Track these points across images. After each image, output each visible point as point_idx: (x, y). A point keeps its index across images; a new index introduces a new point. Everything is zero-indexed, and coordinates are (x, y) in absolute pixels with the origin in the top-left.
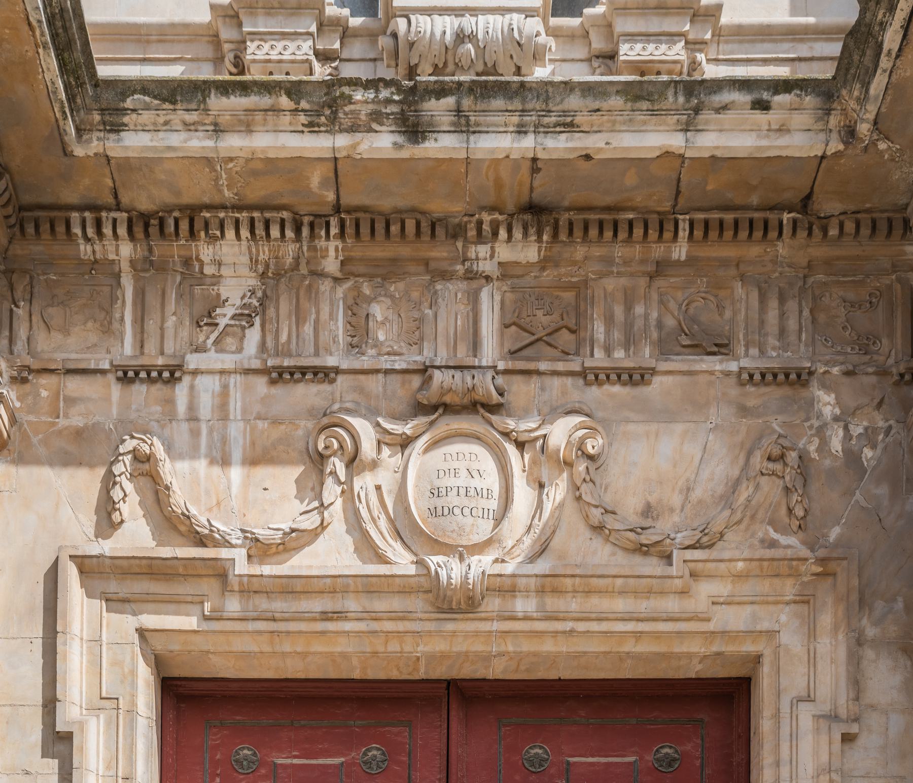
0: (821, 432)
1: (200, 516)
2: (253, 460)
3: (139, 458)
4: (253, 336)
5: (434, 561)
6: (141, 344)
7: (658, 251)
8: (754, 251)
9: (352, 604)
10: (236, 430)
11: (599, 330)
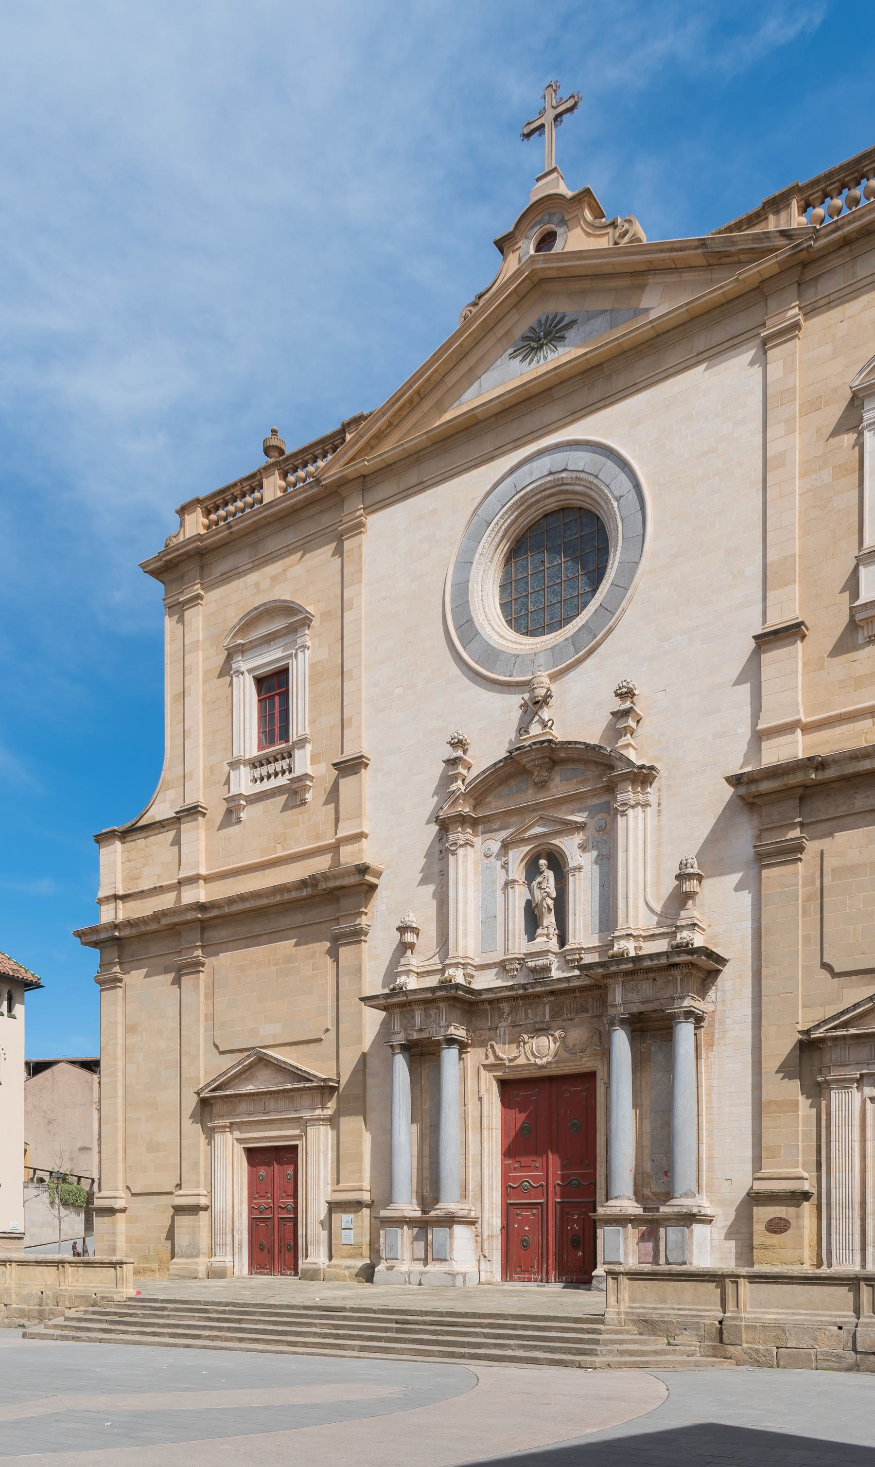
0: (604, 1026)
1: (500, 1054)
2: (509, 1043)
3: (491, 1045)
4: (510, 1018)
5: (537, 1060)
6: (491, 1023)
7: (574, 995)
8: (591, 993)
9: (526, 1068)
10: (507, 1037)
11: (565, 1011)
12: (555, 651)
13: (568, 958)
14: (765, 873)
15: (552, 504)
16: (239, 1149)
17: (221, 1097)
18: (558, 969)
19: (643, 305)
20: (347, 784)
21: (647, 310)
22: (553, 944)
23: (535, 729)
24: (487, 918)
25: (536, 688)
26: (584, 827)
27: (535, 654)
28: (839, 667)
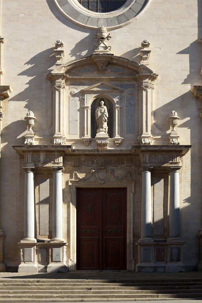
12: (108, 21)
13: (116, 142)
18: (110, 147)
22: (107, 136)
23: (101, 49)
24: (72, 120)
25: (103, 32)
26: (123, 92)
27: (98, 19)
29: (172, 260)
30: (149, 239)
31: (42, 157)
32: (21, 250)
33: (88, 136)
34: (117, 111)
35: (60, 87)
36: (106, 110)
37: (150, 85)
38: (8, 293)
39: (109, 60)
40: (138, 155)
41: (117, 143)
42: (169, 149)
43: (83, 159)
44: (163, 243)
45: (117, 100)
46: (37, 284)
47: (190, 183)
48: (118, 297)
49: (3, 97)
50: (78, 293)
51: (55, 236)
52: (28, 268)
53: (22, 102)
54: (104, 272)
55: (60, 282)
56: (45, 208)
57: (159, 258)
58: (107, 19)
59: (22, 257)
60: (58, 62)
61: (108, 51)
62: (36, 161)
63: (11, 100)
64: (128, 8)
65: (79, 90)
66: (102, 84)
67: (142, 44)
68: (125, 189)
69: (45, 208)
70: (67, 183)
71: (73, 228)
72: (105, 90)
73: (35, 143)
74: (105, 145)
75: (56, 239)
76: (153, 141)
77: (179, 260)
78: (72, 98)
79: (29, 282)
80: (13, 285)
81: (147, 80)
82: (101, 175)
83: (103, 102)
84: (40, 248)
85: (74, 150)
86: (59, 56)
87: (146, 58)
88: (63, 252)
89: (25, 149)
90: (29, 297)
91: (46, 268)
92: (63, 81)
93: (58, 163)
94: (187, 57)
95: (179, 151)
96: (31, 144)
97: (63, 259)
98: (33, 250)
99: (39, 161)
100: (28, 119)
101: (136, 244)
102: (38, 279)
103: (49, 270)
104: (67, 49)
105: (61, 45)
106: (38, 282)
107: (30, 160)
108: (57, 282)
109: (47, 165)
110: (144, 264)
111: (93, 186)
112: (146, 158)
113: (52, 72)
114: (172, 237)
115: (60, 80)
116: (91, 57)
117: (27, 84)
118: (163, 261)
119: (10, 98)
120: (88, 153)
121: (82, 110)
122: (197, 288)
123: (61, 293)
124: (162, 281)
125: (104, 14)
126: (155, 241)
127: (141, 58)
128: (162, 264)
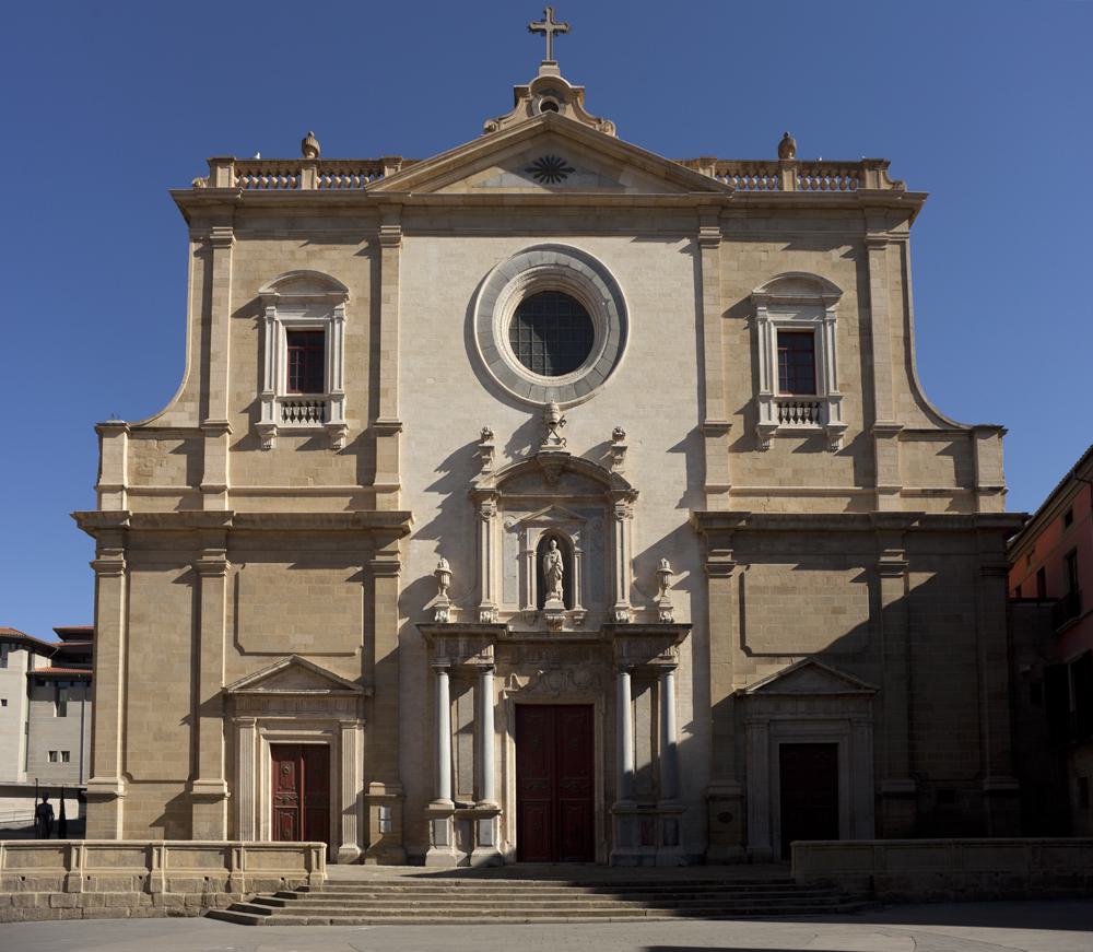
12: (562, 392)
14: (711, 581)
15: (552, 286)
16: (265, 746)
17: (248, 694)
19: (621, 181)
20: (381, 442)
21: (623, 187)
22: (561, 606)
23: (551, 444)
28: (746, 458)
29: (666, 844)
30: (629, 802)
31: (462, 645)
32: (431, 823)
33: (532, 607)
34: (576, 559)
35: (488, 514)
36: (560, 558)
37: (627, 512)
38: (411, 906)
39: (562, 463)
40: (610, 643)
41: (577, 620)
42: (659, 630)
43: (525, 650)
44: (652, 811)
45: (577, 538)
46: (457, 888)
47: (691, 695)
48: (583, 914)
49: (401, 532)
50: (521, 906)
51: (484, 797)
52: (441, 857)
53: (431, 541)
54: (562, 865)
55: (492, 884)
56: (468, 740)
57: (645, 842)
58: (559, 387)
59: (431, 835)
60: (486, 468)
61: (560, 448)
62: (452, 654)
63: (414, 537)
64: (591, 368)
65: (518, 520)
66: (553, 509)
67: (614, 435)
68: (591, 707)
69: (468, 740)
70: (501, 694)
71: (511, 780)
72: (557, 519)
73: (452, 619)
74: (559, 623)
75: (484, 801)
76: (633, 616)
77: (677, 844)
78: (506, 535)
79: (444, 884)
80: (418, 891)
81: (622, 502)
82: (554, 680)
83: (555, 542)
84: (460, 819)
85: (511, 633)
86: (487, 457)
87: (620, 461)
88: (495, 827)
89: (435, 630)
90: (444, 914)
91: (469, 857)
92: (494, 503)
93: (486, 658)
94: (682, 457)
95: (673, 634)
96: (445, 620)
97: (495, 840)
98: (449, 822)
99: (457, 654)
100: (440, 573)
101: (610, 812)
102: (457, 880)
103: (474, 862)
104: (499, 443)
105: (490, 436)
106: (457, 884)
107: (443, 652)
108: (487, 884)
109: (469, 662)
110: (622, 852)
111: (540, 702)
112: (621, 648)
113: (477, 486)
114: (665, 798)
115: (488, 501)
116: (535, 458)
117: (439, 507)
118: (653, 844)
119: (412, 534)
120: (532, 638)
121: (523, 556)
122: (706, 897)
123: (493, 906)
124: (652, 884)
125: (555, 378)
126: (639, 807)
127: (612, 461)
128: (649, 851)
